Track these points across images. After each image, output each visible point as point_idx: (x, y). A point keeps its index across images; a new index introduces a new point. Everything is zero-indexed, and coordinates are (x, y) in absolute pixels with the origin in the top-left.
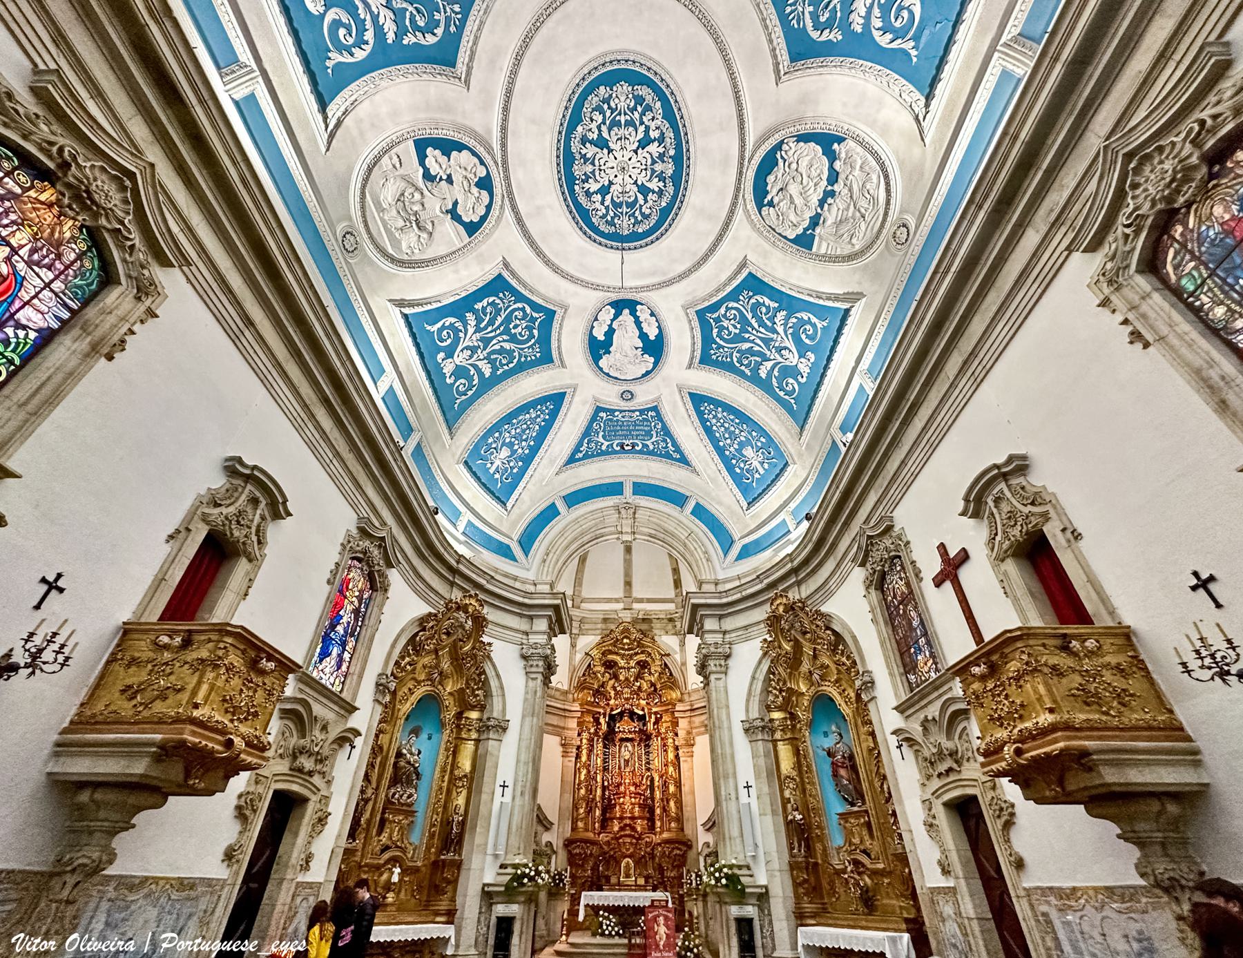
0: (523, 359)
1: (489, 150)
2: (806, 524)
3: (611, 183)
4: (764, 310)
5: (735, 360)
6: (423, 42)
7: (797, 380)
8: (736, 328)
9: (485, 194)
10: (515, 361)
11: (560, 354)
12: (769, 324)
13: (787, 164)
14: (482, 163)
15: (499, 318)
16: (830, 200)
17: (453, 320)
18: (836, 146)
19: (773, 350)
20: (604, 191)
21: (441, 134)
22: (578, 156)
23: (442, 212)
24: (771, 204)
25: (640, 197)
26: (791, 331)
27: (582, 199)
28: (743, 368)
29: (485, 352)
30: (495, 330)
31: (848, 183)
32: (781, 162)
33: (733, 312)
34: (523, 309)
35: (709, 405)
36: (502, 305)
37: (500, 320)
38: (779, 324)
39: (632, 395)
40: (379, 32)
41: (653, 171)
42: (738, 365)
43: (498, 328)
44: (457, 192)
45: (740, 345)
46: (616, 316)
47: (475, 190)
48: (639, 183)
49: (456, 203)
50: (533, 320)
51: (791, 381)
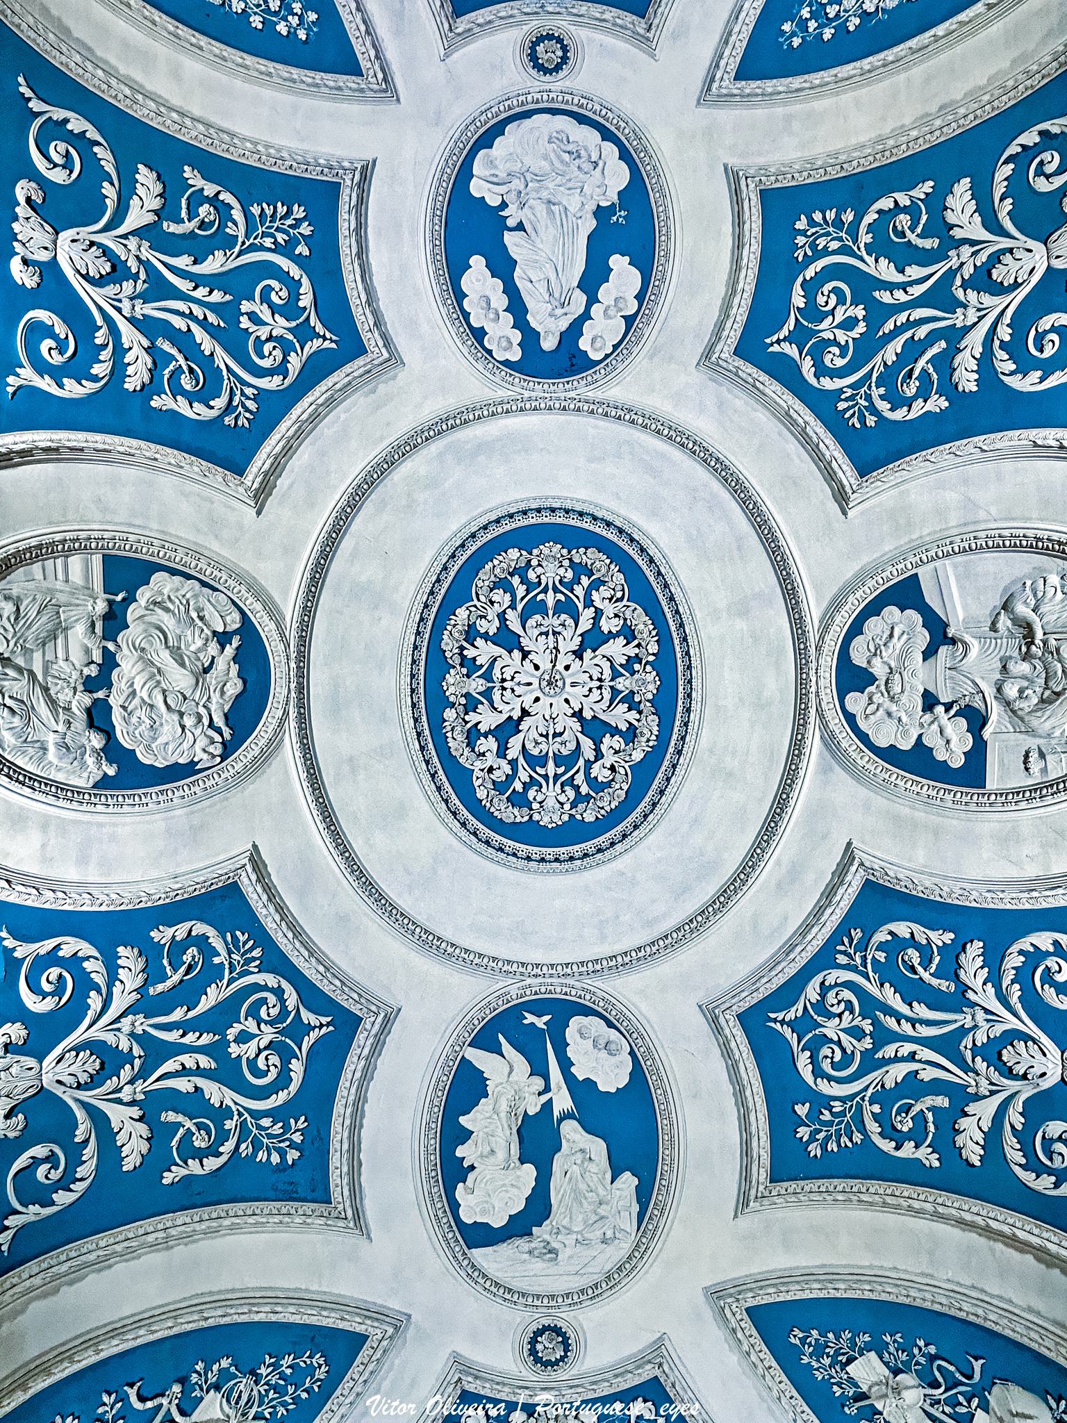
0: (849, 217)
1: (830, 741)
3: (578, 654)
4: (186, 383)
5: (237, 214)
6: (916, 928)
7: (42, 182)
8: (252, 317)
9: (859, 656)
10: (870, 217)
11: (739, 220)
12: (167, 347)
13: (206, 721)
14: (850, 718)
15: (891, 358)
16: (93, 671)
17: (1015, 382)
18: (111, 771)
19: (133, 265)
20: (593, 640)
21: (926, 787)
22: (647, 707)
23: (964, 643)
24: (223, 639)
25: (514, 624)
26: (100, 337)
27: (642, 622)
28: (210, 189)
29: (954, 263)
30: (909, 325)
31: (62, 717)
32: (219, 721)
33: (266, 363)
34: (821, 370)
35: (292, 34)
36: (876, 393)
37: (890, 353)
38: (136, 350)
39: (533, 57)
40: (994, 963)
41: (487, 676)
42: (226, 197)
43: (897, 331)
44: (919, 676)
45: (231, 265)
46: (575, 329)
47: (878, 669)
48: (517, 654)
49: (929, 653)
50: (799, 337)
51: (58, 176)
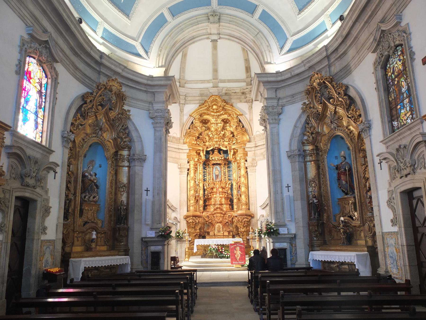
2: (339, 24)
